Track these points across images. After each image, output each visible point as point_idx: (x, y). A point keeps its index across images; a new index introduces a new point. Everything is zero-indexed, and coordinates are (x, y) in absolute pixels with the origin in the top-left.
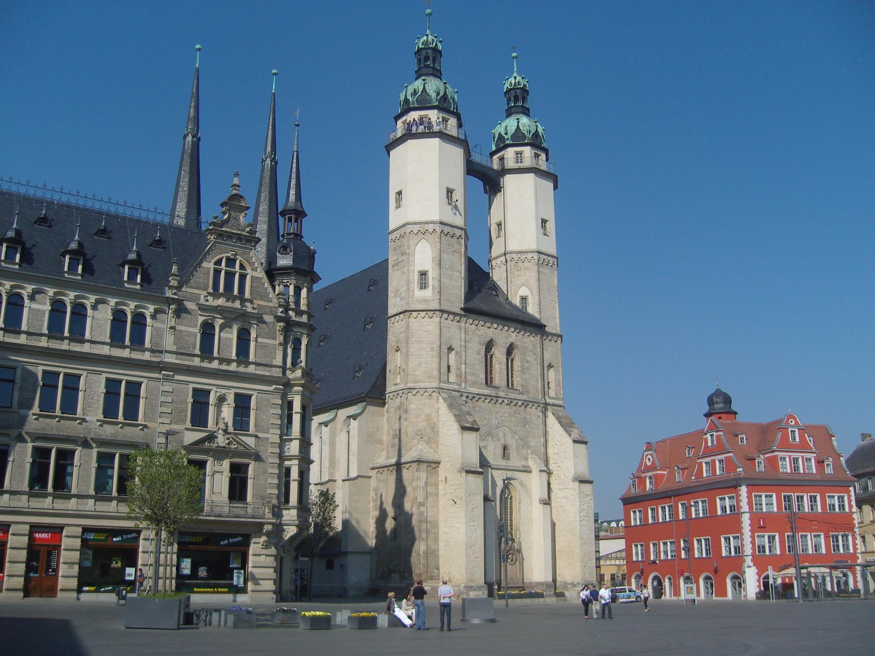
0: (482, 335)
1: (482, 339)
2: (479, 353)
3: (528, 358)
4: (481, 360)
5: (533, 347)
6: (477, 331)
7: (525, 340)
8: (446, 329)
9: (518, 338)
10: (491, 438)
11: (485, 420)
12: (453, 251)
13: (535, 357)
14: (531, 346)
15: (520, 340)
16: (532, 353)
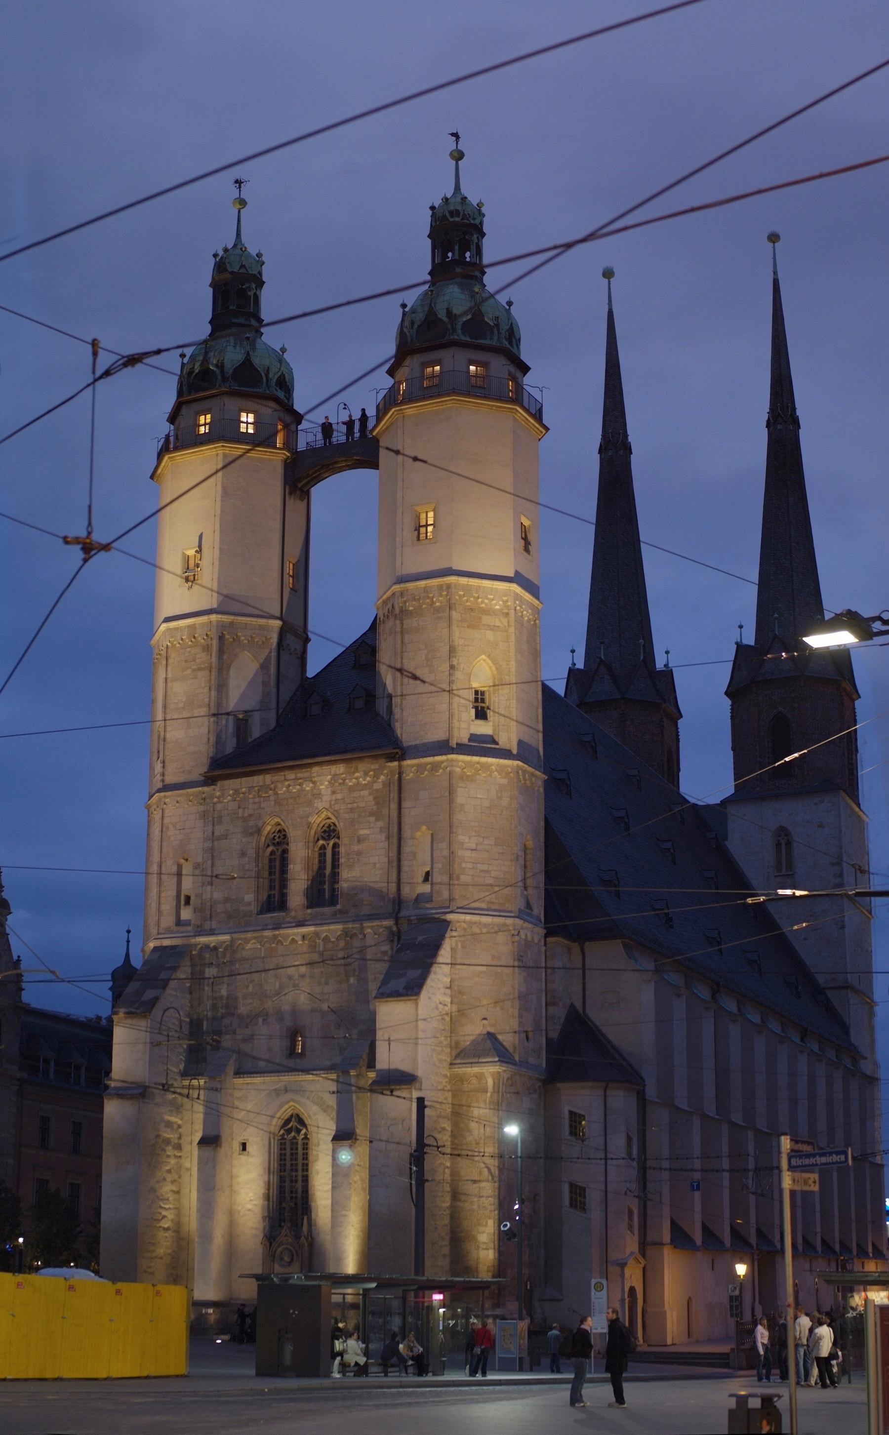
0: (251, 815)
1: (251, 823)
2: (243, 854)
3: (362, 832)
4: (247, 867)
5: (377, 804)
6: (241, 811)
7: (355, 794)
8: (174, 826)
9: (339, 796)
10: (264, 1020)
11: (251, 986)
12: (194, 670)
13: (380, 824)
14: (373, 803)
15: (343, 799)
16: (373, 819)
